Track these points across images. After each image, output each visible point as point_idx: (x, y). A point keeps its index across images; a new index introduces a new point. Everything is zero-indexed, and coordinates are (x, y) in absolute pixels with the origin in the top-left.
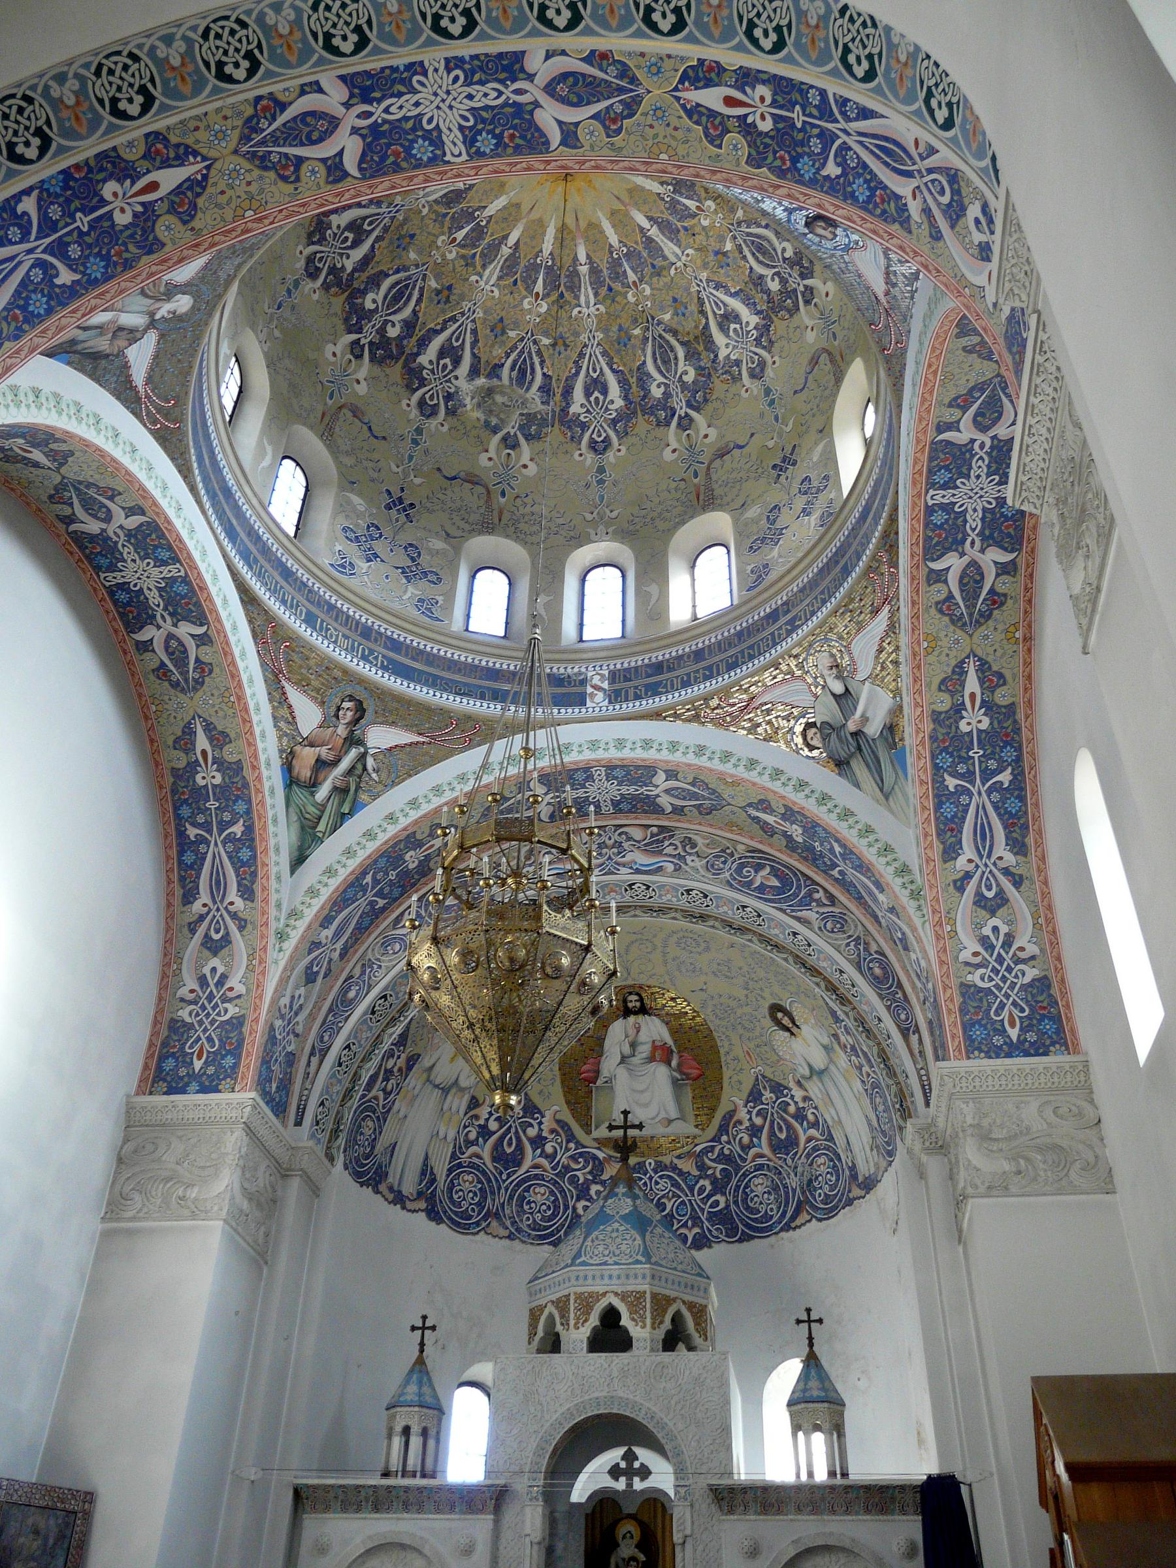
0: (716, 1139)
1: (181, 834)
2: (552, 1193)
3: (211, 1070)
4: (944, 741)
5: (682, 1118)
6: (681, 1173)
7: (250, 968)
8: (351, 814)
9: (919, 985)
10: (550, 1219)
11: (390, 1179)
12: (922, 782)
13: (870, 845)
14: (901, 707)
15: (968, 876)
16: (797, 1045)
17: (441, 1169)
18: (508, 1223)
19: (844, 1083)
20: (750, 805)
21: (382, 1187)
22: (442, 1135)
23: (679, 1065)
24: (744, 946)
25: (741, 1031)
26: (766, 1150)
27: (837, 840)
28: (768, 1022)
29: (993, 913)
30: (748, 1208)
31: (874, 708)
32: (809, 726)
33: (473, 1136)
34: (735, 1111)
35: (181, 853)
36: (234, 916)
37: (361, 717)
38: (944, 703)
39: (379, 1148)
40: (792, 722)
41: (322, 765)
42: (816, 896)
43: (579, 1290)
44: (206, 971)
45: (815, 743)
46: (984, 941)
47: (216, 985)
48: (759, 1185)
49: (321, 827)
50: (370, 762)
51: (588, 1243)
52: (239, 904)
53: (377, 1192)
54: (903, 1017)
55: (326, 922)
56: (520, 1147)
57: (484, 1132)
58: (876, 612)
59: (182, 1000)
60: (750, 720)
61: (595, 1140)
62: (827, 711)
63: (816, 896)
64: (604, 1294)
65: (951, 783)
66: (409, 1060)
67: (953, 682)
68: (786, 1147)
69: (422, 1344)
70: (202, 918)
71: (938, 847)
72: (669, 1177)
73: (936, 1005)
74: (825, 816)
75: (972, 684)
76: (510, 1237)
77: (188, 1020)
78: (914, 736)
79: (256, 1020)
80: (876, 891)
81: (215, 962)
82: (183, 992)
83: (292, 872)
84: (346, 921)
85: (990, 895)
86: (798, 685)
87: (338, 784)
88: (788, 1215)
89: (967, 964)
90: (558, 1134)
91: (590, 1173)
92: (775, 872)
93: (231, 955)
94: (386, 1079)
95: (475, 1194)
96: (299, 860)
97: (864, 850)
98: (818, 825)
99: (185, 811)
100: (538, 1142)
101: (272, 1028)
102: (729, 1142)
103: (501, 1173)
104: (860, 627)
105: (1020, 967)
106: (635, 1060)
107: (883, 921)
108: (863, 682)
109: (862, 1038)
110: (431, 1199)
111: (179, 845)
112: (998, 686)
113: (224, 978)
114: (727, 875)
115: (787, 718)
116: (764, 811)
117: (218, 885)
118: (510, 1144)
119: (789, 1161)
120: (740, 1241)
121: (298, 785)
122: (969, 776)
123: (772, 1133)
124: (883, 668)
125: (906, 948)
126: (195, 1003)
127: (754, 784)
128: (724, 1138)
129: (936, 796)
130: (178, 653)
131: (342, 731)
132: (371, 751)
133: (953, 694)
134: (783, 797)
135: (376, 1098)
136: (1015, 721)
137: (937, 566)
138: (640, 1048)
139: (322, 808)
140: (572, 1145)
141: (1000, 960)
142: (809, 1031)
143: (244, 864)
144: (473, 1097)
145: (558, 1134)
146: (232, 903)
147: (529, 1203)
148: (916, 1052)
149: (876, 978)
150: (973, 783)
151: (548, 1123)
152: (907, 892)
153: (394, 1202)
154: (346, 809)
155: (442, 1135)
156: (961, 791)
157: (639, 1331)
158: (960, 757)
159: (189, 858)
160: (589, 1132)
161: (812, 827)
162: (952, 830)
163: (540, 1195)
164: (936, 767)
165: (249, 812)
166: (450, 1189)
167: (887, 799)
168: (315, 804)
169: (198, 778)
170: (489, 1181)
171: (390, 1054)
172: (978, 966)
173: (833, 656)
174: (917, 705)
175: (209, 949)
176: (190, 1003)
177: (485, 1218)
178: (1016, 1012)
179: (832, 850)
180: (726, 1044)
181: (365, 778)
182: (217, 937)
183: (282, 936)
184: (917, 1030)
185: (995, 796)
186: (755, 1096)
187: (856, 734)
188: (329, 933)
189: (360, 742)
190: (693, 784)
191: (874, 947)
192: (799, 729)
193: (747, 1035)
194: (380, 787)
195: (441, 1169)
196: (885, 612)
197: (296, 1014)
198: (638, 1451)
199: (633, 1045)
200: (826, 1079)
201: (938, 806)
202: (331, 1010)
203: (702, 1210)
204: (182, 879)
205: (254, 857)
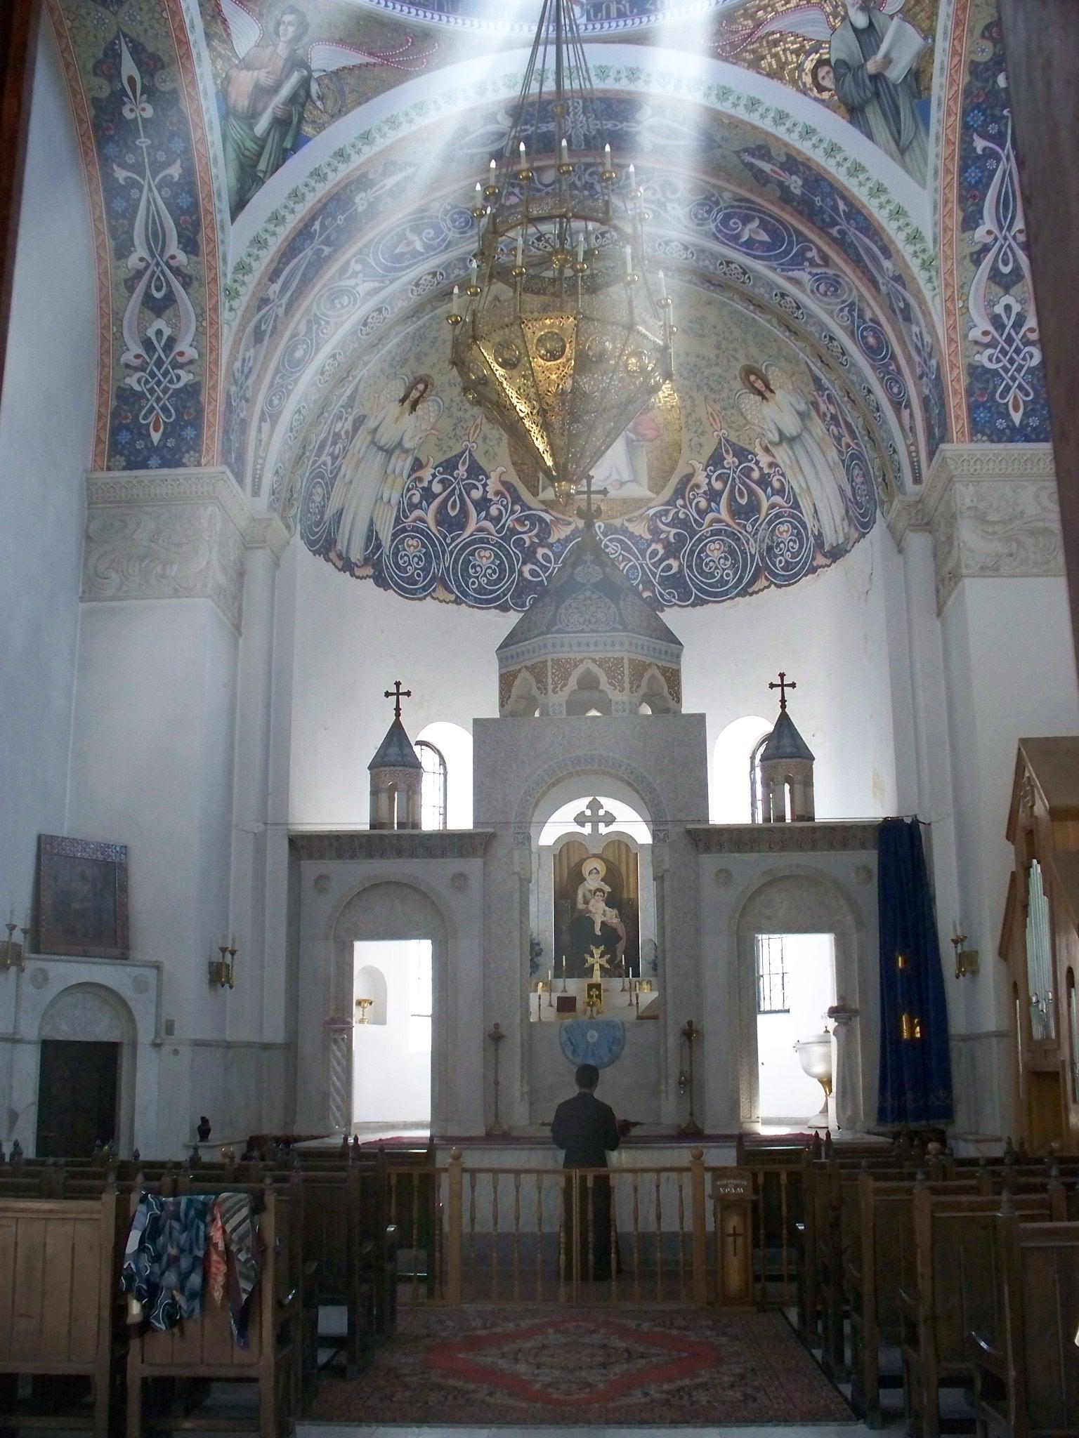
1: (108, 177)
2: (497, 555)
3: (171, 442)
4: (978, 96)
5: (636, 481)
6: (632, 536)
7: (200, 331)
8: (296, 147)
9: (917, 359)
10: (496, 582)
11: (339, 547)
12: (948, 142)
13: (881, 207)
14: (932, 51)
15: (986, 249)
16: (768, 409)
17: (385, 532)
18: (455, 590)
19: (818, 452)
20: (746, 150)
21: (332, 555)
22: (385, 499)
24: (724, 304)
25: (707, 392)
26: (724, 515)
27: (844, 198)
28: (737, 385)
29: (1007, 290)
30: (702, 572)
31: (900, 47)
32: (821, 63)
33: (416, 499)
34: (692, 475)
36: (177, 271)
39: (329, 513)
40: (802, 57)
42: (809, 255)
43: (555, 656)
44: (151, 333)
45: (828, 83)
46: (997, 322)
47: (164, 350)
48: (715, 551)
49: (262, 166)
50: (314, 88)
51: (562, 611)
52: (182, 258)
53: (328, 560)
54: (895, 390)
55: (274, 275)
56: (464, 511)
57: (428, 495)
59: (128, 366)
60: (754, 51)
61: (543, 502)
62: (842, 47)
63: (809, 255)
64: (581, 661)
65: (980, 144)
66: (355, 421)
68: (746, 514)
71: (958, 215)
72: (619, 541)
73: (938, 382)
74: (833, 170)
76: (457, 601)
77: (137, 388)
78: (944, 88)
79: (214, 387)
80: (881, 257)
81: (160, 324)
82: (128, 357)
83: (233, 219)
84: (293, 273)
85: (1006, 270)
86: (814, 14)
87: (279, 114)
88: (745, 581)
89: (976, 343)
90: (503, 496)
91: (537, 536)
92: (764, 225)
93: (177, 316)
94: (334, 443)
95: (420, 559)
96: (239, 205)
97: (875, 212)
98: (824, 179)
100: (483, 504)
101: (228, 396)
102: (684, 506)
105: (1027, 349)
107: (883, 288)
108: (892, 17)
109: (847, 408)
110: (377, 565)
111: (106, 190)
113: (170, 343)
114: (712, 226)
115: (797, 53)
116: (762, 158)
119: (749, 529)
120: (693, 605)
121: (235, 116)
123: (732, 498)
125: (908, 319)
126: (142, 369)
127: (755, 128)
128: (680, 502)
129: (962, 158)
132: (316, 75)
134: (787, 145)
135: (325, 464)
140: (518, 508)
141: (1009, 341)
142: (783, 397)
144: (417, 460)
145: (503, 496)
146: (173, 257)
147: (474, 567)
148: (907, 427)
149: (870, 348)
150: (1002, 146)
151: (493, 485)
152: (919, 262)
153: (343, 570)
154: (288, 144)
155: (385, 499)
156: (989, 154)
158: (993, 116)
159: (120, 205)
160: (535, 494)
161: (817, 181)
162: (974, 197)
163: (485, 558)
164: (966, 128)
165: (187, 151)
166: (395, 554)
169: (126, 111)
170: (434, 545)
171: (339, 417)
172: (987, 346)
174: (955, 53)
175: (152, 309)
176: (136, 369)
177: (430, 584)
178: (1020, 396)
179: (835, 208)
181: (309, 107)
182: (158, 295)
183: (232, 294)
184: (908, 406)
186: (716, 460)
187: (877, 78)
191: (868, 315)
192: (809, 65)
193: (713, 396)
194: (326, 118)
195: (385, 532)
197: (247, 377)
198: (602, 800)
200: (798, 447)
201: (963, 169)
202: (277, 371)
203: (654, 575)
204: (113, 231)
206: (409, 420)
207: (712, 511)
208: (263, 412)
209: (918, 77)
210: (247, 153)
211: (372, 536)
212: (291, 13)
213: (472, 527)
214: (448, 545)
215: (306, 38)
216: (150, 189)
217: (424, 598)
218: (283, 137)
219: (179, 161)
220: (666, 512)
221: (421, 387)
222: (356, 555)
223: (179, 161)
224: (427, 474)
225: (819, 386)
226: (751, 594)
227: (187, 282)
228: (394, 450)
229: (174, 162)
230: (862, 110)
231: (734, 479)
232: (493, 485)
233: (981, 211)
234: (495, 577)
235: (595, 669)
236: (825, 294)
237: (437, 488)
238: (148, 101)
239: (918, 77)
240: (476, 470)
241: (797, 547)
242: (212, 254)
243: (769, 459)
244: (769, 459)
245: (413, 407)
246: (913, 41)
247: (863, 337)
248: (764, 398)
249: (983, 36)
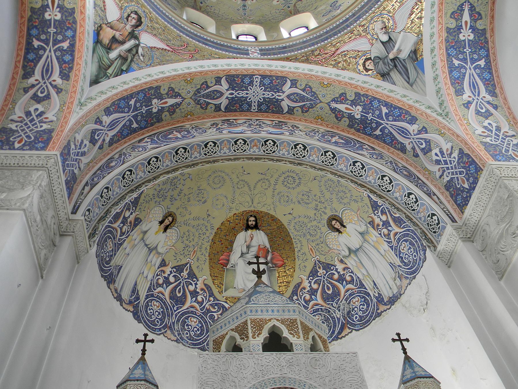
1: (29, 44)
2: (200, 322)
4: (452, 43)
11: (116, 285)
15: (469, 103)
17: (143, 293)
18: (176, 334)
21: (112, 286)
22: (145, 275)
23: (272, 259)
25: (309, 237)
26: (320, 301)
28: (325, 229)
33: (161, 281)
34: (301, 283)
35: (27, 52)
36: (55, 87)
37: (140, 25)
38: (452, 24)
40: (358, 59)
41: (114, 40)
43: (253, 317)
49: (110, 71)
50: (140, 50)
52: (59, 82)
54: (425, 189)
56: (184, 295)
57: (167, 281)
62: (377, 50)
64: (270, 320)
65: (456, 63)
68: (332, 298)
69: (144, 351)
70: (33, 86)
71: (452, 90)
75: (466, 17)
76: (177, 341)
82: (15, 117)
86: (364, 40)
87: (122, 54)
88: (336, 332)
90: (205, 291)
93: (49, 104)
95: (159, 313)
96: (95, 82)
99: (34, 32)
100: (194, 294)
102: (297, 300)
103: (174, 306)
108: (400, 33)
110: (136, 307)
111: (26, 49)
112: (478, 19)
117: (47, 71)
118: (179, 292)
119: (335, 304)
122: (465, 60)
124: (412, 22)
129: (449, 67)
131: (129, 28)
132: (142, 45)
133: (457, 20)
136: (486, 38)
138: (252, 249)
139: (112, 62)
140: (212, 299)
142: (350, 228)
143: (65, 62)
144: (163, 260)
145: (205, 291)
146: (54, 81)
147: (188, 325)
151: (200, 285)
154: (124, 68)
155: (145, 275)
156: (461, 67)
157: (296, 341)
158: (460, 51)
159: (31, 56)
160: (221, 292)
162: (458, 83)
163: (193, 322)
164: (449, 55)
165: (74, 37)
166: (147, 306)
167: (412, 86)
168: (108, 59)
170: (167, 309)
173: (384, 22)
180: (299, 245)
181: (136, 57)
185: (478, 71)
186: (314, 273)
188: (107, 120)
189: (136, 38)
191: (400, 165)
193: (312, 238)
194: (143, 65)
195: (143, 293)
199: (248, 247)
201: (450, 72)
204: (24, 67)
205: (73, 60)
206: (162, 236)
207: (313, 300)
208: (87, 182)
210: (103, 62)
211: (134, 290)
212: (135, 14)
213: (188, 304)
214: (175, 311)
215: (140, 28)
216: (50, 51)
217: (160, 334)
218: (122, 64)
219: (68, 41)
221: (170, 219)
222: (126, 295)
223: (68, 41)
224: (168, 270)
226: (341, 338)
227: (59, 91)
228: (153, 249)
229: (66, 40)
230: (389, 74)
231: (324, 281)
232: (200, 285)
233: (463, 88)
234: (198, 332)
235: (278, 324)
236: (377, 159)
237: (172, 279)
238: (59, 12)
240: (192, 275)
241: (365, 307)
243: (343, 266)
244: (343, 266)
245: (165, 230)
247: (401, 172)
248: (340, 232)
249: (451, 17)
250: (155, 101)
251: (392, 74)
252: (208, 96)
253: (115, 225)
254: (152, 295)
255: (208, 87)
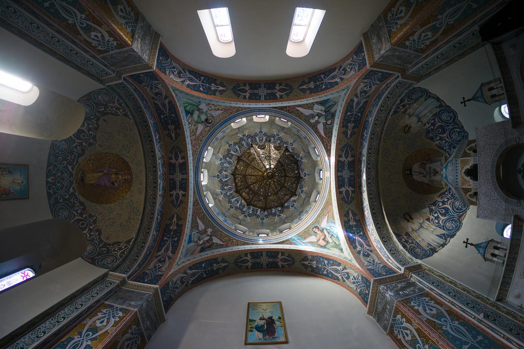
0: (445, 150)
1: (325, 275)
5: (440, 160)
16: (414, 126)
26: (445, 135)
33: (437, 221)
35: (329, 277)
49: (337, 243)
52: (341, 267)
57: (437, 218)
58: (298, 110)
62: (322, 120)
67: (304, 91)
70: (342, 278)
96: (341, 250)
104: (302, 113)
106: (425, 173)
117: (336, 271)
118: (442, 211)
130: (285, 260)
131: (319, 232)
137: (279, 97)
159: (330, 276)
187: (325, 112)
189: (323, 229)
190: (343, 151)
196: (297, 108)
209: (321, 103)
211: (440, 236)
213: (448, 206)
220: (448, 152)
222: (441, 241)
225: (396, 112)
239: (321, 103)
242: (341, 260)
246: (316, 106)
250: (351, 223)
251: (332, 112)
252: (348, 198)
253: (408, 247)
254: (443, 226)
255: (344, 197)
